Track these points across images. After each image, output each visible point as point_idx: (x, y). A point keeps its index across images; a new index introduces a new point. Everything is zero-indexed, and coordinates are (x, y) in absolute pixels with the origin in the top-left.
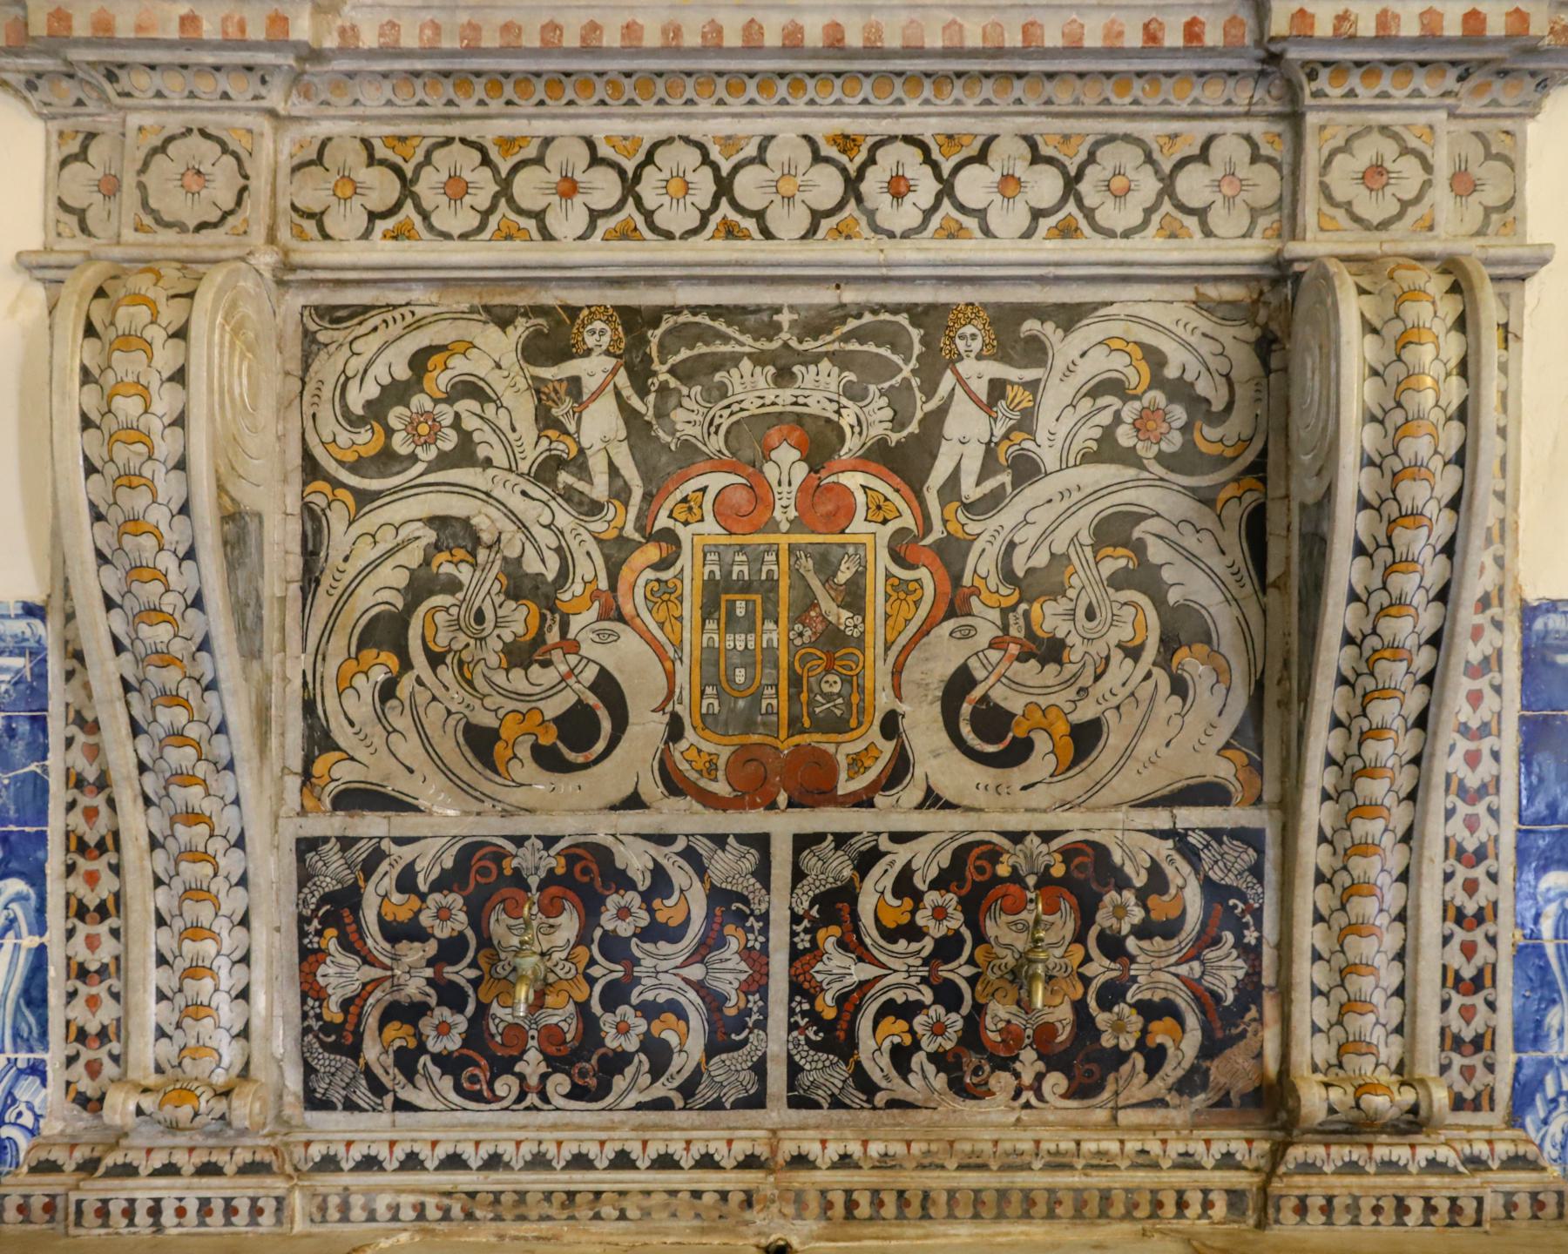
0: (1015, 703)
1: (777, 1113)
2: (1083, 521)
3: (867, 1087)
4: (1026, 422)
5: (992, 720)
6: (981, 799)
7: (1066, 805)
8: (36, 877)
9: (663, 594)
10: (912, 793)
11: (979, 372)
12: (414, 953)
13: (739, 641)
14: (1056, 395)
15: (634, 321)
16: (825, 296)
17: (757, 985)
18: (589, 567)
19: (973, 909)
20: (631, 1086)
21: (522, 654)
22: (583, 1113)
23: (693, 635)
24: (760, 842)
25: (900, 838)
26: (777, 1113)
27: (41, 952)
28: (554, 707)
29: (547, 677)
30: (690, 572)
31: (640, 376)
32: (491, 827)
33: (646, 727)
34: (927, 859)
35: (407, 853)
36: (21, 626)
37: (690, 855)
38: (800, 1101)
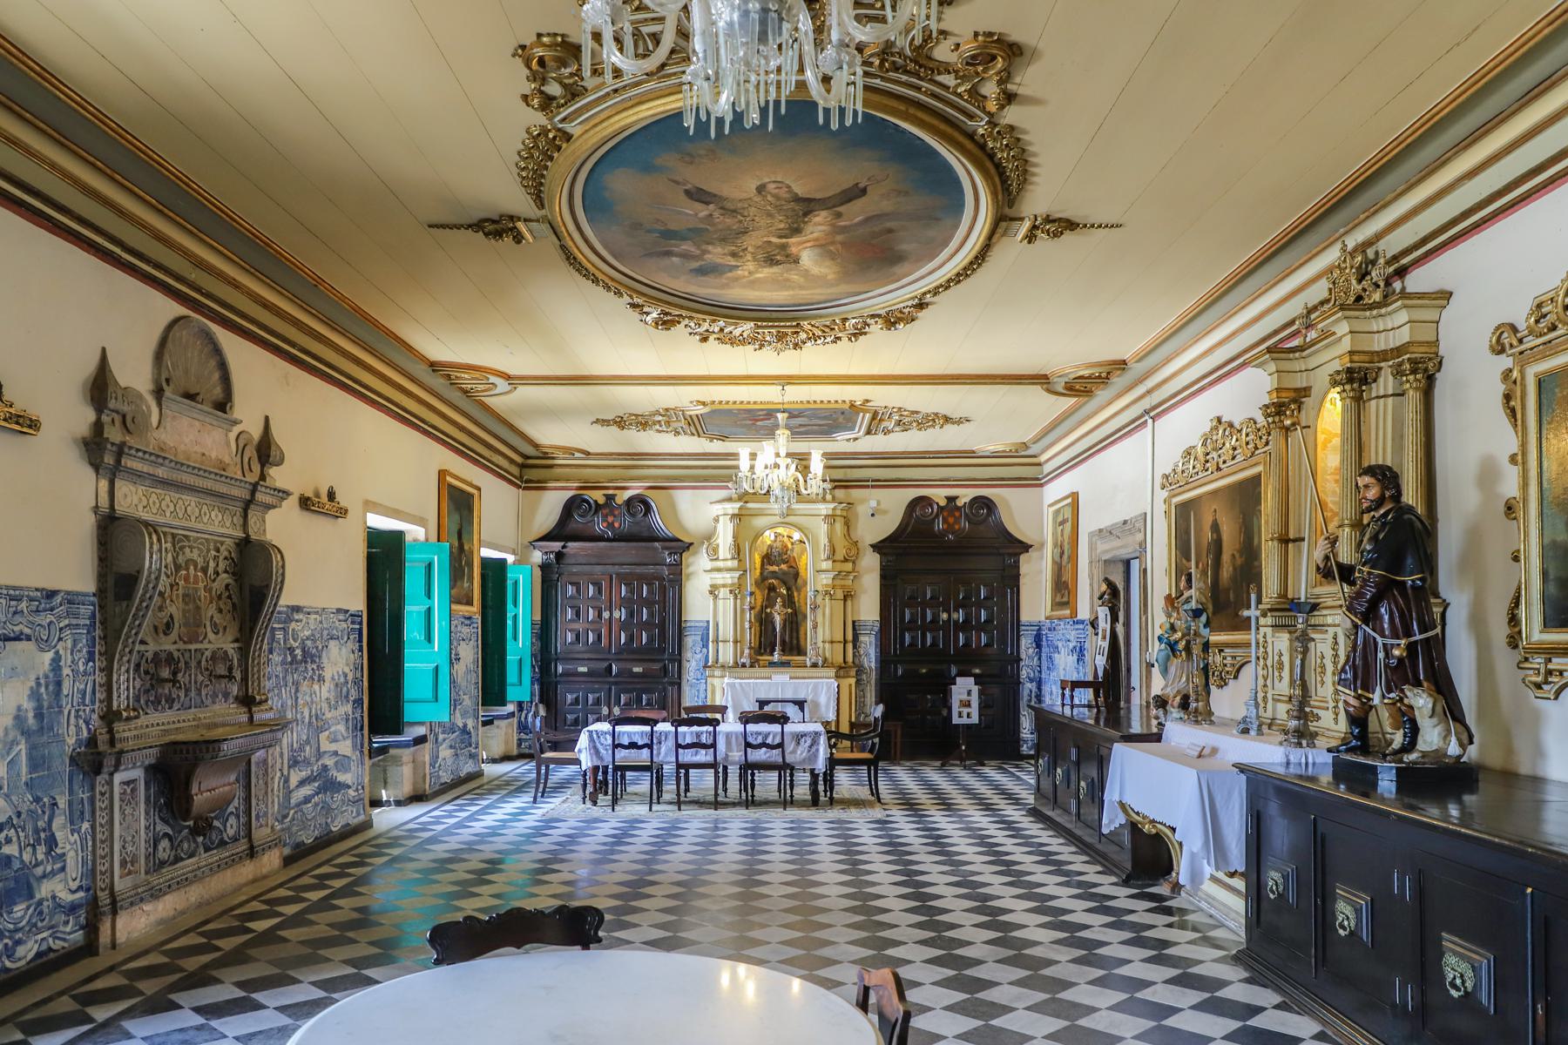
1: (193, 710)
4: (217, 565)
5: (216, 625)
8: (94, 662)
11: (213, 553)
12: (148, 677)
14: (221, 558)
17: (190, 682)
20: (176, 706)
22: (169, 712)
23: (181, 605)
24: (190, 651)
28: (165, 621)
29: (164, 614)
30: (181, 591)
32: (157, 648)
34: (208, 654)
35: (146, 654)
37: (182, 654)
38: (195, 707)
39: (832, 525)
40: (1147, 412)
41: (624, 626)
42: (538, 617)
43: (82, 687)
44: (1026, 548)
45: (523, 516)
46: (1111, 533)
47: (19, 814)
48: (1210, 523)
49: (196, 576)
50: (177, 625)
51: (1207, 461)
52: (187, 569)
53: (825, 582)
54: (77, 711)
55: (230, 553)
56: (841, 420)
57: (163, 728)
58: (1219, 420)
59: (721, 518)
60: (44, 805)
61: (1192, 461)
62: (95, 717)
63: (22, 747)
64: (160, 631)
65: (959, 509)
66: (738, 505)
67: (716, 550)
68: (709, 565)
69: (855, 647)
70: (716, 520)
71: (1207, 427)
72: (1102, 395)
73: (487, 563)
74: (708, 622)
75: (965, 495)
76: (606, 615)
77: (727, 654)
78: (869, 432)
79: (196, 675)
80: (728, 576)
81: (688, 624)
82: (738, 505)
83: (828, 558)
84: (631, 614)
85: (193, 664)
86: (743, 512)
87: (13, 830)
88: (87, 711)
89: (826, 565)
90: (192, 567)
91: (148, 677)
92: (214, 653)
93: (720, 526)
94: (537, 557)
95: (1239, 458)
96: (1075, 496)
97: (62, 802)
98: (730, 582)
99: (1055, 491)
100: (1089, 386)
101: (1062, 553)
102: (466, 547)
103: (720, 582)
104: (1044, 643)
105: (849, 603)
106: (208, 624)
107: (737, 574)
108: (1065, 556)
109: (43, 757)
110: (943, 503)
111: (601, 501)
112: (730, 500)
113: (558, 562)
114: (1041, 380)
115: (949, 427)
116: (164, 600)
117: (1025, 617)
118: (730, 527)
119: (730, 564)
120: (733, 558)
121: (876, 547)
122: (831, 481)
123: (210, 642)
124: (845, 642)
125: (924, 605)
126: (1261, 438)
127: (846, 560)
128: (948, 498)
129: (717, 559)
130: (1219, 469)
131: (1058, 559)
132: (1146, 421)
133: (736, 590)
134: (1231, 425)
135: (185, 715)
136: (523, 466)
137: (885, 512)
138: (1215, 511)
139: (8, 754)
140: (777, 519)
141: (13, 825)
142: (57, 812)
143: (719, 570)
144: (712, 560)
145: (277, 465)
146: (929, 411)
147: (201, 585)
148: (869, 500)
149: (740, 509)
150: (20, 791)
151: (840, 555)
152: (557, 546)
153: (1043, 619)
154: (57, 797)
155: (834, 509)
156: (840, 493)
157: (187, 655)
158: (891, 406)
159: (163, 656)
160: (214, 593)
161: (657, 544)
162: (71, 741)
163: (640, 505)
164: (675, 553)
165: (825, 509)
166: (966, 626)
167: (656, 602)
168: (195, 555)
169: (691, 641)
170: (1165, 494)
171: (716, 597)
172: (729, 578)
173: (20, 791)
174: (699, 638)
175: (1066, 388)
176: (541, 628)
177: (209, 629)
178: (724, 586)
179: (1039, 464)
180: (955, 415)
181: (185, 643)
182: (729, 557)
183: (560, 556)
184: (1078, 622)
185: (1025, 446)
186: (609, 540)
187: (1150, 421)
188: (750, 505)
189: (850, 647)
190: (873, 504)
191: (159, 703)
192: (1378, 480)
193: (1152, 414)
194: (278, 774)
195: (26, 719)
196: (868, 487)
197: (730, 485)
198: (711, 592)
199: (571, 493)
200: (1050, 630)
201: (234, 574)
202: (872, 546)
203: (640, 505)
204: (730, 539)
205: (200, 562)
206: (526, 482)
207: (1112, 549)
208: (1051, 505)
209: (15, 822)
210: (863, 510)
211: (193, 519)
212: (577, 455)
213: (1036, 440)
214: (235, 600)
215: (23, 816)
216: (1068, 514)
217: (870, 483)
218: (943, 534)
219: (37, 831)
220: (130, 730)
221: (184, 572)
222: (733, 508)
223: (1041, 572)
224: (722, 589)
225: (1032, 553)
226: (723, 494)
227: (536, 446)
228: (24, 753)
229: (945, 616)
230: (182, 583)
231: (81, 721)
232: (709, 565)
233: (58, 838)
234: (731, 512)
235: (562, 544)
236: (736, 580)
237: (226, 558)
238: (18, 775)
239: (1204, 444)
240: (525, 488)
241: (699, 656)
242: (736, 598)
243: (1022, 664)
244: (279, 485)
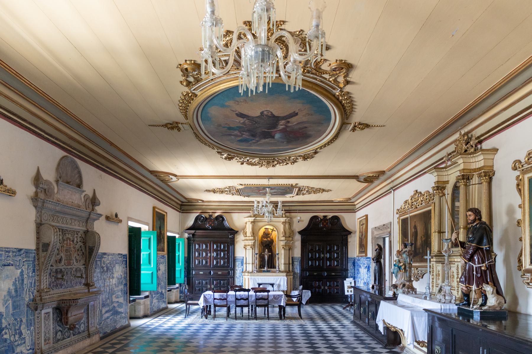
1: (69, 288)
2: (79, 246)
3: (72, 286)
4: (77, 239)
5: (77, 260)
7: (79, 266)
8: (35, 273)
9: (64, 250)
11: (76, 235)
12: (54, 277)
13: (67, 254)
17: (68, 279)
18: (60, 248)
19: (76, 273)
21: (58, 254)
22: (61, 289)
23: (65, 253)
24: (68, 268)
27: (35, 279)
28: (59, 258)
29: (59, 256)
30: (65, 249)
32: (57, 268)
34: (74, 269)
36: (34, 251)
37: (65, 269)
38: (70, 287)
39: (285, 226)
40: (392, 188)
41: (216, 258)
42: (186, 255)
43: (31, 281)
44: (350, 233)
45: (182, 222)
46: (379, 228)
47: (9, 324)
48: (413, 226)
49: (70, 243)
50: (63, 260)
51: (412, 205)
52: (67, 241)
53: (282, 244)
54: (29, 289)
55: (82, 235)
56: (288, 190)
57: (59, 294)
58: (417, 191)
59: (248, 223)
60: (18, 321)
61: (407, 205)
62: (35, 291)
63: (10, 302)
64: (58, 262)
65: (327, 220)
66: (253, 218)
67: (246, 233)
68: (244, 238)
69: (292, 266)
70: (246, 223)
71: (412, 194)
72: (376, 182)
73: (169, 237)
74: (243, 257)
75: (330, 215)
76: (209, 255)
77: (250, 268)
78: (297, 194)
79: (70, 277)
80: (250, 242)
81: (237, 258)
82: (253, 218)
83: (284, 236)
84: (217, 255)
85: (69, 273)
86: (255, 221)
87: (7, 330)
88: (33, 289)
89: (283, 238)
90: (69, 240)
91: (54, 277)
93: (247, 226)
94: (186, 235)
95: (424, 204)
96: (367, 216)
97: (24, 320)
98: (250, 244)
99: (360, 214)
100: (372, 179)
101: (362, 235)
102: (162, 232)
103: (247, 244)
104: (356, 265)
105: (291, 251)
106: (74, 259)
107: (253, 241)
108: (363, 236)
109: (17, 305)
110: (322, 218)
111: (208, 217)
112: (250, 216)
113: (193, 237)
114: (356, 177)
115: (324, 193)
117: (350, 256)
118: (251, 225)
119: (251, 238)
120: (252, 236)
121: (300, 233)
122: (285, 210)
123: (75, 265)
124: (289, 264)
125: (316, 252)
126: (431, 197)
127: (289, 237)
128: (323, 216)
129: (246, 236)
130: (416, 208)
131: (361, 237)
132: (391, 191)
133: (253, 247)
134: (421, 193)
135: (66, 290)
136: (181, 205)
137: (302, 221)
138: (415, 222)
139: (5, 304)
140: (267, 223)
141: (7, 328)
142: (22, 323)
143: (247, 240)
144: (245, 237)
145: (98, 206)
146: (318, 187)
147: (72, 246)
148: (298, 217)
149: (254, 220)
150: (10, 317)
151: (287, 235)
152: (193, 231)
153: (356, 257)
154: (22, 318)
155: (286, 220)
156: (288, 214)
157: (67, 270)
158: (305, 186)
159: (59, 270)
160: (76, 249)
161: (226, 231)
162: (27, 299)
163: (221, 219)
164: (232, 234)
165: (283, 220)
166: (330, 259)
167: (225, 251)
168: (70, 236)
169: (238, 263)
170: (398, 216)
171: (246, 249)
172: (251, 243)
173: (10, 317)
174: (240, 263)
175: (364, 180)
176: (188, 259)
177: (74, 261)
178: (249, 245)
179: (355, 205)
180: (327, 189)
181: (66, 266)
182: (250, 236)
183: (193, 235)
184: (368, 258)
185: (350, 199)
186: (210, 230)
187: (393, 191)
188: (257, 218)
189: (291, 266)
190: (299, 218)
191: (57, 286)
192: (474, 213)
193: (393, 189)
195: (12, 292)
196: (297, 212)
197: (251, 212)
198: (244, 247)
199: (198, 214)
200: (358, 260)
201: (83, 242)
202: (298, 232)
203: (221, 219)
204: (251, 230)
205: (71, 238)
206: (183, 210)
207: (380, 234)
208: (358, 219)
209: (8, 327)
210: (295, 220)
212: (199, 201)
213: (353, 197)
214: (83, 251)
215: (11, 325)
216: (364, 222)
217: (298, 211)
218: (322, 228)
219: (15, 330)
220: (47, 295)
221: (66, 242)
222: (252, 219)
223: (355, 241)
224: (248, 246)
225: (352, 235)
226: (248, 214)
227: (186, 198)
228: (11, 303)
229: (322, 256)
230: (65, 246)
231: (30, 293)
232: (244, 238)
233: (23, 332)
234: (251, 221)
235: (194, 231)
236: (253, 244)
237: (80, 237)
238: (9, 311)
239: (411, 199)
240: (182, 213)
241: (240, 268)
242: (252, 249)
243: (349, 271)
244: (99, 212)
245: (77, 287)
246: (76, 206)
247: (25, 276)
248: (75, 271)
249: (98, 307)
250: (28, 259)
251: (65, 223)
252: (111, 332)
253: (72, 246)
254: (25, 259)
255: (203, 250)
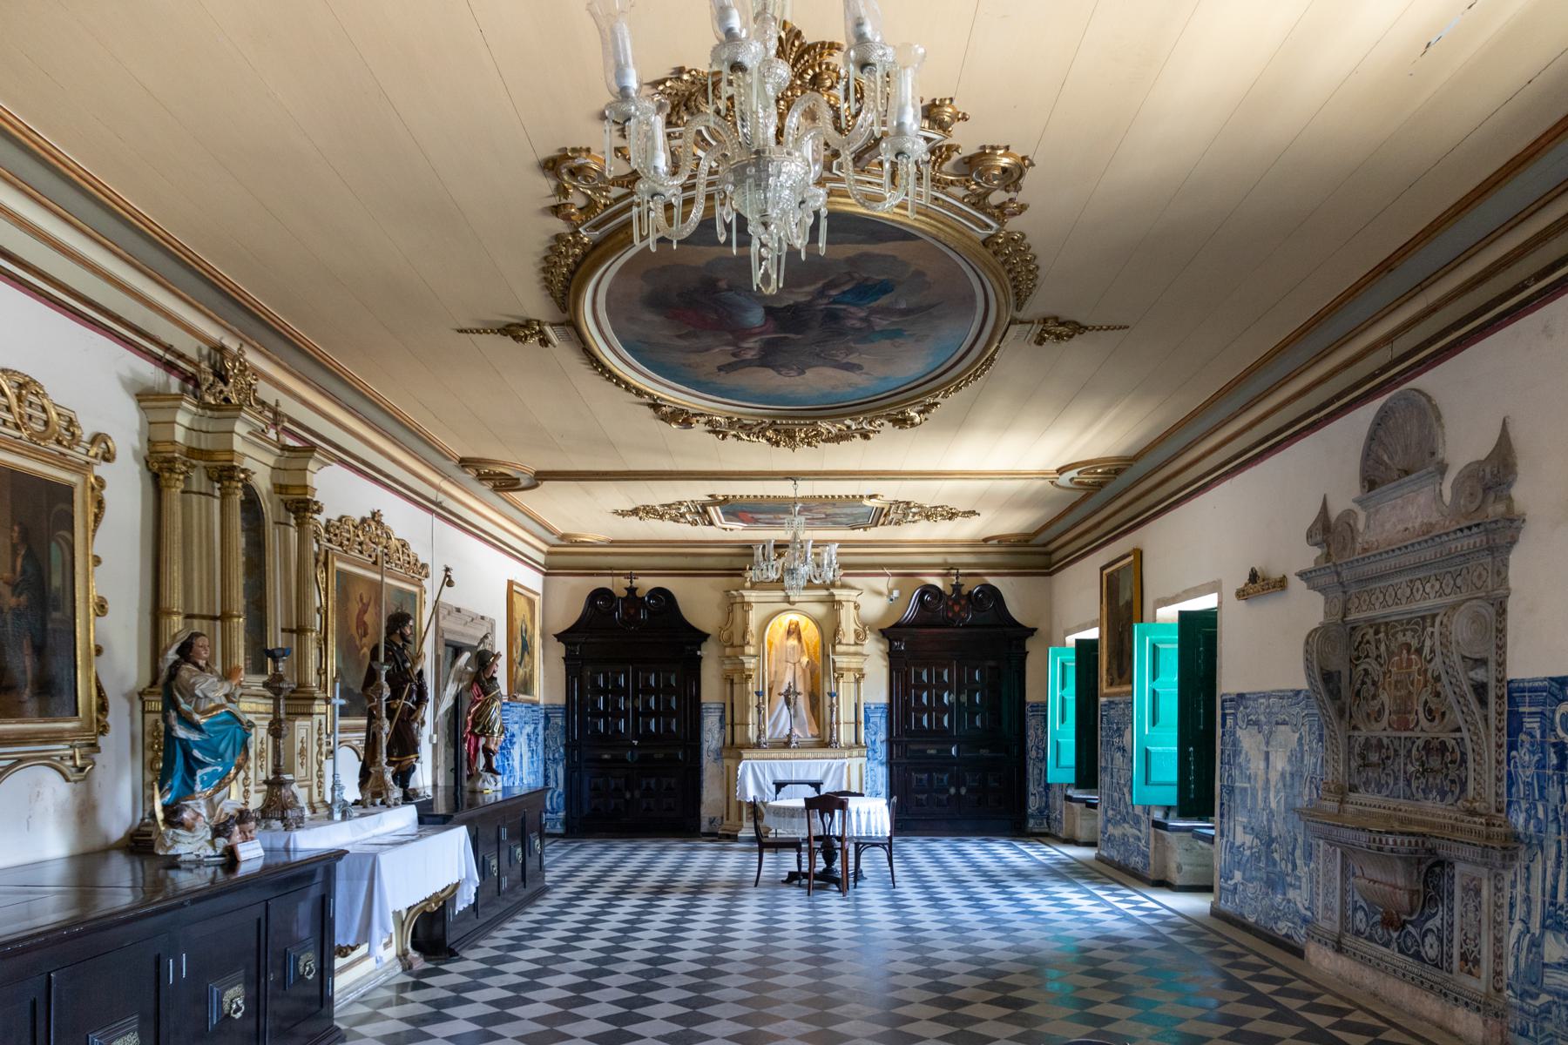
0: (1433, 708)
5: (1430, 711)
6: (1428, 729)
7: (1440, 731)
9: (1390, 683)
10: (1419, 728)
13: (1398, 694)
15: (1387, 624)
16: (1409, 616)
17: (1399, 771)
18: (1381, 678)
20: (1385, 792)
22: (1378, 797)
24: (1400, 738)
25: (1418, 738)
26: (1402, 800)
28: (1377, 709)
30: (1394, 678)
31: (1387, 636)
32: (1369, 734)
33: (1387, 712)
34: (1420, 743)
38: (1405, 798)
49: (1409, 660)
50: (1387, 712)
57: (1360, 808)
64: (1372, 718)
79: (1405, 764)
85: (1402, 752)
90: (1405, 652)
92: (1427, 743)
106: (1421, 710)
116: (1377, 688)
123: (1422, 730)
135: (1393, 803)
147: (1415, 668)
157: (1396, 743)
159: (1374, 742)
160: (1429, 675)
177: (1421, 716)
181: (1395, 730)
194: (1518, 926)
205: (1415, 643)
211: (1404, 601)
230: (1394, 670)
245: (1429, 804)
246: (1418, 536)
247: (1306, 748)
248: (1424, 747)
249: (1520, 910)
250: (1311, 711)
251: (1390, 603)
252: (1284, 939)
253: (1415, 668)
254: (1306, 712)
255: (927, 687)
